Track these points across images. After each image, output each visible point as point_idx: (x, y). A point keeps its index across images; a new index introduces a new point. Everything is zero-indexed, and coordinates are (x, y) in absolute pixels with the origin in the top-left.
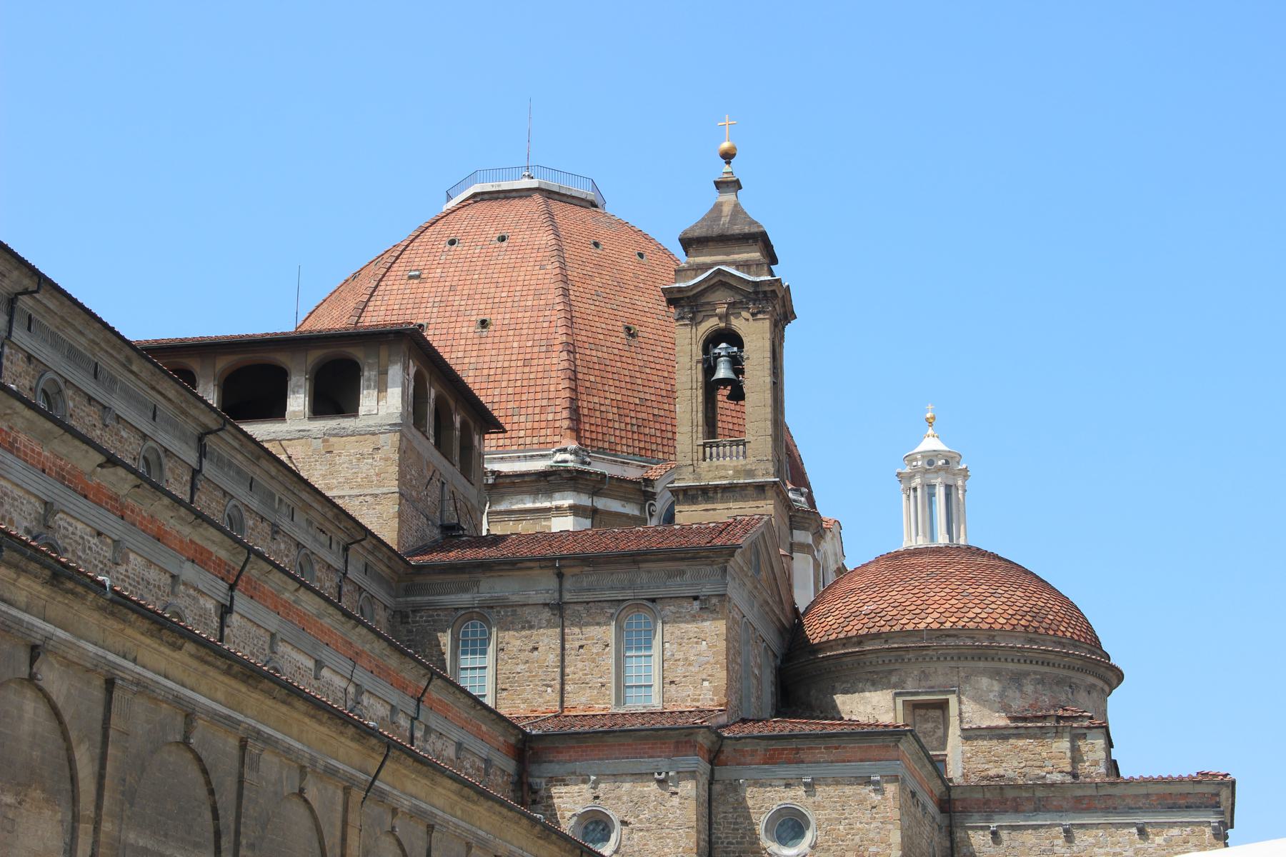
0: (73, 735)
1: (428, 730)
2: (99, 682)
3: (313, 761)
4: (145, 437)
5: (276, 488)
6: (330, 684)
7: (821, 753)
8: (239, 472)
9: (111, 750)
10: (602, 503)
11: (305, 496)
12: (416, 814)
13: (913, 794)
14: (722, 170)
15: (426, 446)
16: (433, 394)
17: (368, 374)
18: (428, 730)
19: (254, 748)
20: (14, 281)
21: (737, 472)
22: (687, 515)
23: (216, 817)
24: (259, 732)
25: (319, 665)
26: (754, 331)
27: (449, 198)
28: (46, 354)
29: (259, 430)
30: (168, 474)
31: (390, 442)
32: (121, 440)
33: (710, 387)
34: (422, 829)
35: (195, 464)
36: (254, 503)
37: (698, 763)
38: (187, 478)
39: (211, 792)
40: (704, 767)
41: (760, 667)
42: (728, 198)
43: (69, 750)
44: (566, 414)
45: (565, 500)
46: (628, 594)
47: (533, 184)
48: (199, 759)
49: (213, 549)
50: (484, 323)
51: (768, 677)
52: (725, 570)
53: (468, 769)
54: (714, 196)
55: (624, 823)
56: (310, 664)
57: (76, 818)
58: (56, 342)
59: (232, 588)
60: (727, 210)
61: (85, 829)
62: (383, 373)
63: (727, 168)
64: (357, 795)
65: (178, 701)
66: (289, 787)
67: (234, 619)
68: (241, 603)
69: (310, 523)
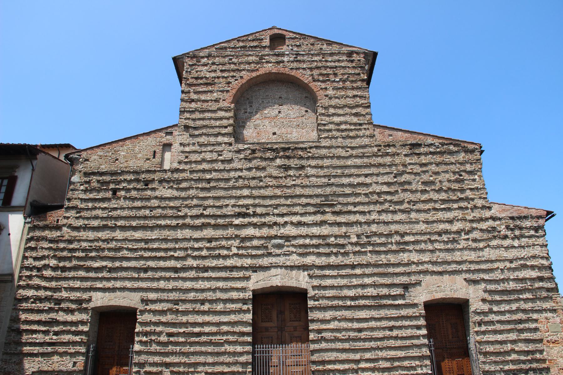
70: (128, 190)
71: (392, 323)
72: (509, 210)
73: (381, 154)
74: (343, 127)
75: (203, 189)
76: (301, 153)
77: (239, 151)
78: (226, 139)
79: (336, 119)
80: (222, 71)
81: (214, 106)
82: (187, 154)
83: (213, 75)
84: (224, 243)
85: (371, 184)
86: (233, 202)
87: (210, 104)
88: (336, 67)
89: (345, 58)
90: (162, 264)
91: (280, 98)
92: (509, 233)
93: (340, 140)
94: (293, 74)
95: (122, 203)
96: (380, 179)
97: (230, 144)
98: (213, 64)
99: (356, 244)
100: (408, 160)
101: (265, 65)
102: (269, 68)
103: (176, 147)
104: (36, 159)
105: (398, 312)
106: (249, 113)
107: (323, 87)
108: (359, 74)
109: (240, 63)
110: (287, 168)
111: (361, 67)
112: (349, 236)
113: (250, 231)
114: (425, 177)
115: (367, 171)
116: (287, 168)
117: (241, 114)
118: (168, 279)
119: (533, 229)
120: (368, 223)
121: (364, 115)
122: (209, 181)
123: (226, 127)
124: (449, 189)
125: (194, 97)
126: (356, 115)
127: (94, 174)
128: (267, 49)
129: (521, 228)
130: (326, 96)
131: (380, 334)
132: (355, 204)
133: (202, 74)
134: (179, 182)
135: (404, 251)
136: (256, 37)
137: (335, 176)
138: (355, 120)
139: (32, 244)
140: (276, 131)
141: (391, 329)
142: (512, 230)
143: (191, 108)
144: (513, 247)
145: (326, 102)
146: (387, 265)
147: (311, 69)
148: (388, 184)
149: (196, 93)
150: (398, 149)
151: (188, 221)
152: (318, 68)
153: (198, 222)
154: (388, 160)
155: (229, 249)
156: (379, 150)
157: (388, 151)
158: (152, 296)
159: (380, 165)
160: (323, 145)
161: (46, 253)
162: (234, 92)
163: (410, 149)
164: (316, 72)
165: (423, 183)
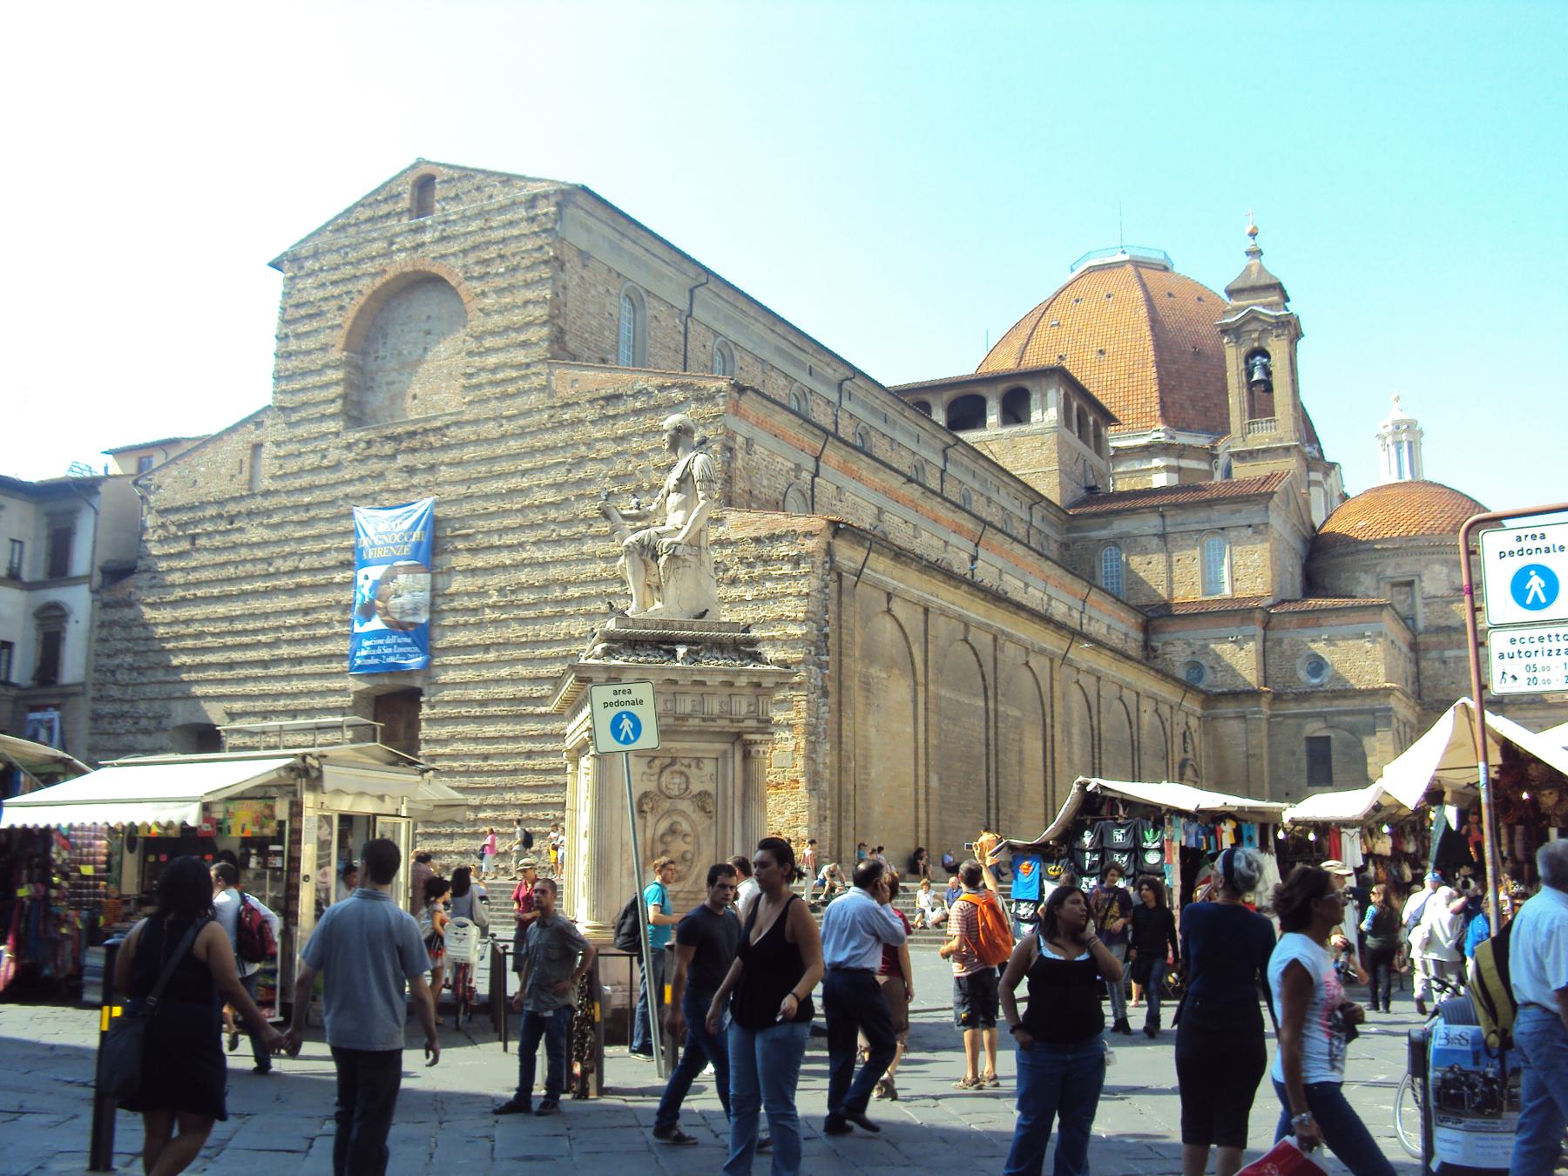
0: (911, 639)
1: (1090, 618)
2: (921, 610)
3: (1032, 644)
4: (914, 453)
5: (988, 475)
6: (1033, 596)
7: (1333, 620)
8: (967, 468)
9: (930, 647)
10: (1184, 463)
11: (1005, 479)
12: (1090, 671)
13: (1393, 642)
14: (1249, 244)
15: (1073, 438)
16: (1075, 405)
17: (1035, 398)
18: (1090, 618)
19: (1001, 640)
20: (844, 372)
21: (1272, 439)
22: (1241, 471)
23: (984, 679)
24: (1003, 632)
25: (1027, 585)
26: (1277, 348)
27: (1072, 270)
28: (860, 413)
29: (968, 436)
30: (928, 474)
31: (1051, 439)
32: (901, 457)
33: (1251, 385)
34: (1094, 679)
35: (942, 467)
36: (976, 486)
37: (1258, 630)
38: (938, 475)
39: (981, 666)
40: (1259, 632)
41: (1292, 566)
42: (1256, 261)
43: (909, 648)
44: (1157, 407)
45: (1157, 462)
46: (1207, 526)
47: (1126, 257)
48: (973, 648)
49: (965, 523)
50: (1102, 352)
51: (1298, 571)
52: (1267, 508)
53: (1115, 640)
55: (1212, 668)
56: (1022, 585)
57: (916, 683)
58: (864, 405)
59: (977, 545)
60: (1254, 269)
61: (921, 689)
62: (1044, 395)
63: (1252, 242)
64: (1058, 662)
66: (1023, 660)
67: (979, 563)
68: (982, 553)
69: (1008, 494)
70: (209, 534)
71: (528, 746)
72: (753, 523)
73: (549, 425)
74: (500, 376)
75: (301, 523)
76: (432, 439)
77: (349, 447)
78: (332, 426)
79: (492, 360)
80: (334, 283)
81: (319, 359)
82: (282, 461)
83: (321, 294)
84: (323, 616)
85: (530, 489)
86: (335, 543)
87: (313, 357)
88: (504, 240)
89: (522, 213)
90: (251, 655)
91: (429, 317)
92: (743, 573)
93: (493, 404)
94: (435, 270)
95: (206, 558)
96: (546, 479)
97: (337, 434)
98: (321, 270)
99: (494, 607)
102: (402, 262)
103: (269, 450)
104: (98, 493)
105: (540, 726)
106: (384, 358)
107: (479, 290)
108: (541, 248)
109: (360, 261)
110: (411, 471)
111: (546, 231)
112: (486, 592)
114: (619, 466)
115: (526, 464)
116: (411, 471)
117: (372, 366)
118: (256, 679)
119: (789, 561)
120: (518, 566)
121: (536, 344)
122: (308, 507)
123: (333, 401)
125: (293, 345)
126: (525, 344)
127: (167, 511)
128: (405, 220)
129: (767, 561)
130: (481, 310)
131: (510, 764)
132: (501, 532)
133: (305, 297)
134: (269, 513)
135: (561, 616)
136: (385, 194)
137: (478, 480)
138: (520, 356)
139: (104, 633)
141: (529, 755)
142: (750, 565)
143: (287, 370)
144: (743, 601)
146: (536, 643)
147: (465, 252)
148: (557, 486)
149: (298, 336)
150: (582, 411)
151: (281, 582)
152: (475, 248)
153: (290, 582)
154: (563, 434)
155: (329, 624)
156: (551, 417)
157: (565, 417)
158: (238, 706)
159: (547, 449)
160: (465, 418)
161: (119, 645)
162: (347, 326)
163: (602, 407)
165: (611, 478)
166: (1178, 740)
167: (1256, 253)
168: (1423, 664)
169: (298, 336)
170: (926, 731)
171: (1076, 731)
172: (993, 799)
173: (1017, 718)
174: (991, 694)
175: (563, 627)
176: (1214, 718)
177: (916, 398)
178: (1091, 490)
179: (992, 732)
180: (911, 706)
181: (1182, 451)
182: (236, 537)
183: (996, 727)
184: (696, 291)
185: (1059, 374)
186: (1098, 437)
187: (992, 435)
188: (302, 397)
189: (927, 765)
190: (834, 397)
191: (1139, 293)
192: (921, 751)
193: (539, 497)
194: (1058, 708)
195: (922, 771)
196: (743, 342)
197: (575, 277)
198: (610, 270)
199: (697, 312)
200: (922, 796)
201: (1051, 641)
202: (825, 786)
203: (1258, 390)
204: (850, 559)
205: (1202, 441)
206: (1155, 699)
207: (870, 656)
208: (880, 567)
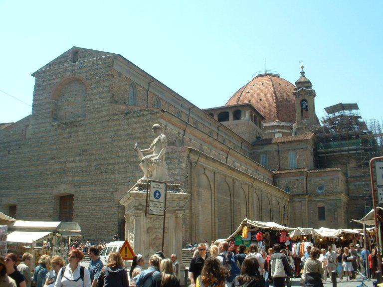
10: (283, 131)
15: (253, 124)
25: (241, 165)
28: (195, 117)
29: (225, 123)
33: (302, 109)
40: (305, 177)
48: (227, 183)
50: (261, 100)
54: (300, 75)
62: (245, 112)
65: (224, 175)
66: (240, 187)
68: (229, 156)
70: (13, 150)
74: (96, 107)
80: (49, 80)
94: (78, 77)
100: (122, 123)
101: (67, 73)
106: (63, 102)
111: (109, 67)
113: (56, 166)
114: (129, 132)
124: (139, 138)
135: (113, 173)
140: (73, 110)
145: (90, 92)
147: (86, 72)
149: (38, 94)
152: (90, 70)
154: (114, 123)
164: (89, 74)
166: (283, 208)
167: (303, 73)
168: (349, 186)
169: (38, 94)
170: (215, 206)
171: (255, 206)
172: (233, 225)
173: (239, 203)
174: (232, 195)
175: (113, 176)
176: (293, 202)
177: (210, 112)
178: (258, 138)
179: (232, 206)
180: (210, 200)
181: (283, 127)
182: (20, 151)
183: (234, 205)
184: (151, 84)
185: (249, 106)
186: (260, 123)
187: (230, 123)
188: (40, 112)
189: (215, 216)
190: (188, 113)
191: (271, 83)
192: (213, 212)
193: (106, 140)
194: (250, 200)
195: (213, 217)
196: (163, 97)
197: (117, 80)
198: (127, 78)
199: (150, 89)
200: (213, 224)
201: (248, 181)
202: (187, 222)
203: (304, 110)
204: (194, 159)
205: (288, 124)
206: (276, 196)
207: (199, 186)
208: (202, 161)
